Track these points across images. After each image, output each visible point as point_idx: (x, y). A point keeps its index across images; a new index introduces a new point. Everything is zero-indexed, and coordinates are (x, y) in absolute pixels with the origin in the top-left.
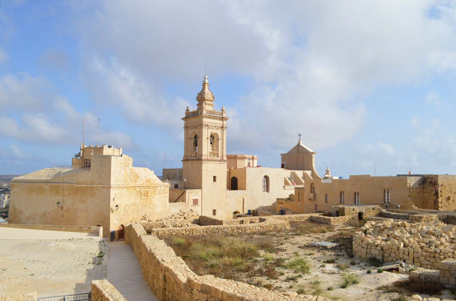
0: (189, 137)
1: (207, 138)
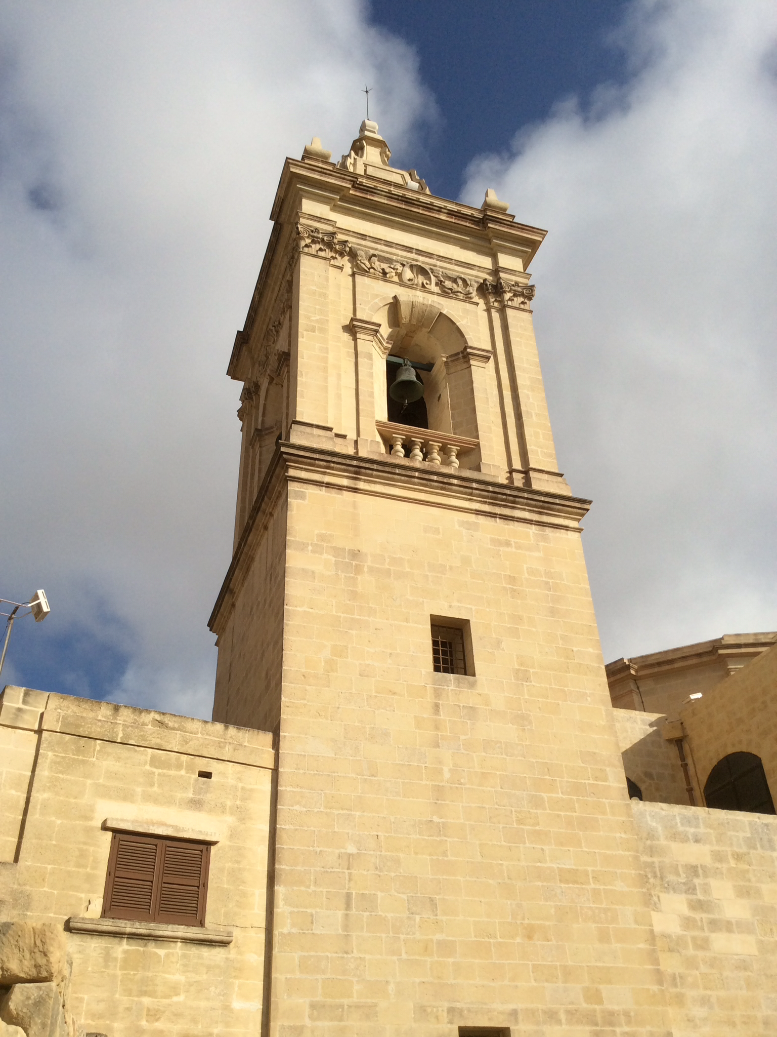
1: (352, 329)
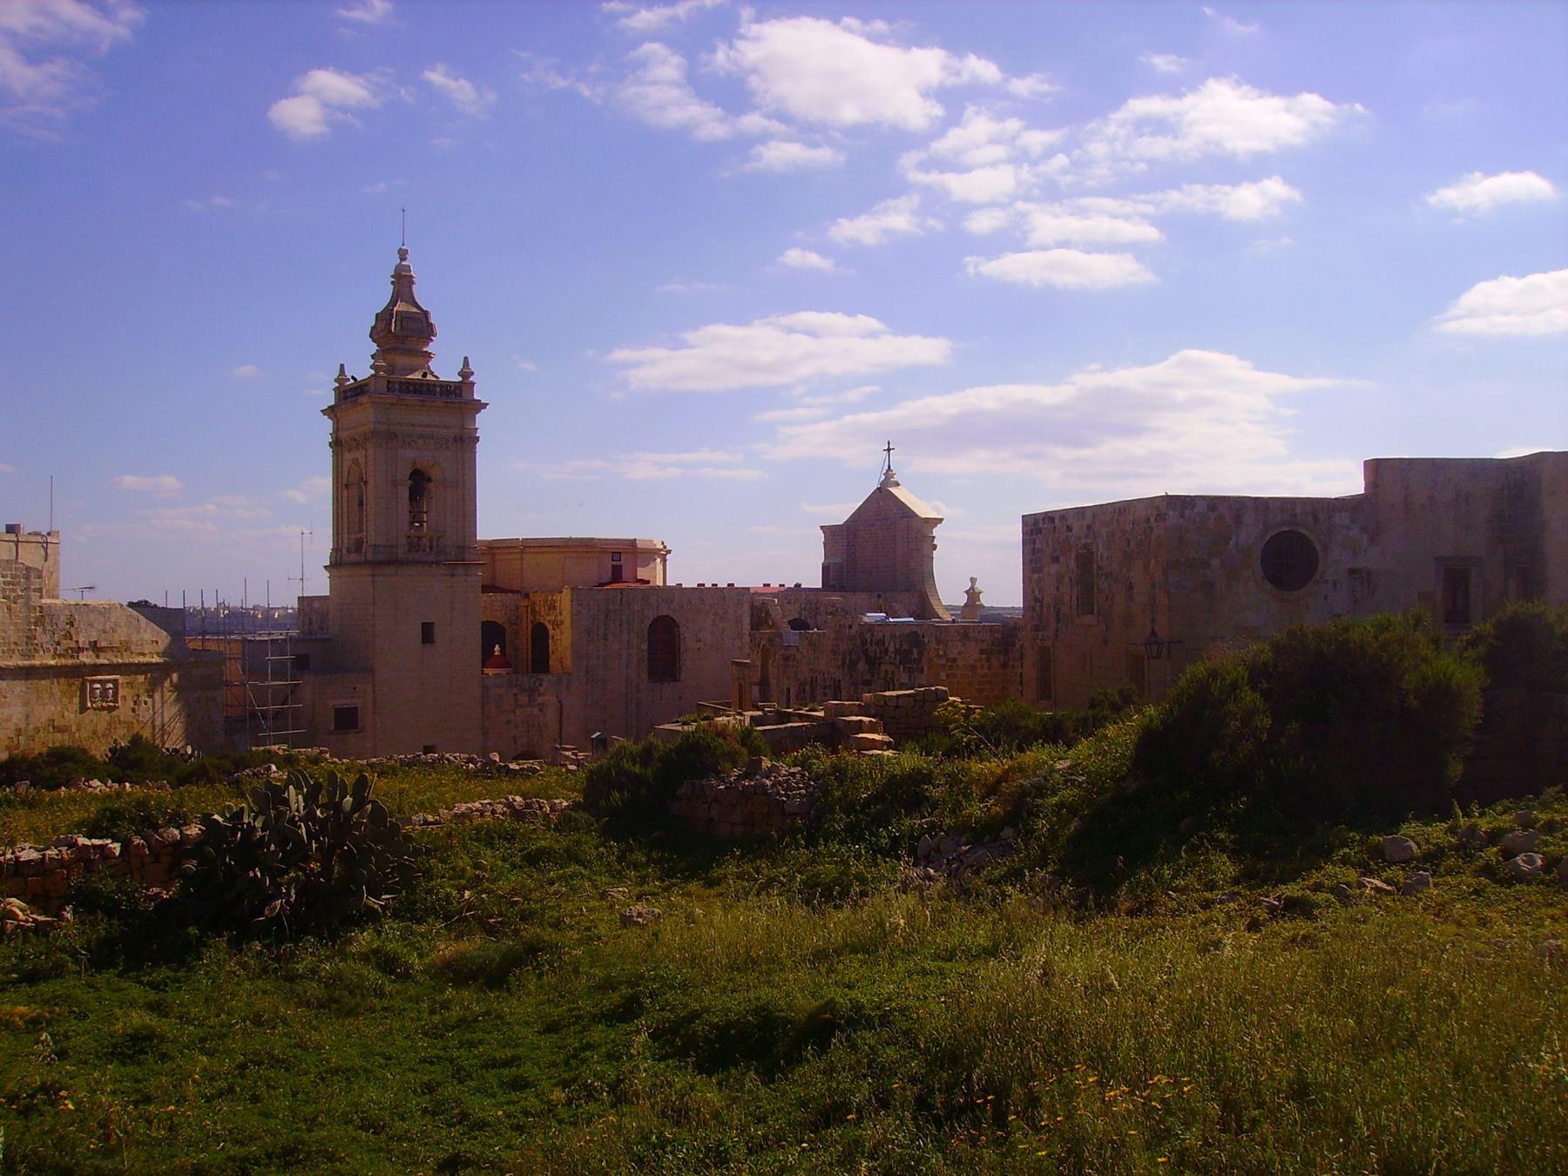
0: (345, 482)
